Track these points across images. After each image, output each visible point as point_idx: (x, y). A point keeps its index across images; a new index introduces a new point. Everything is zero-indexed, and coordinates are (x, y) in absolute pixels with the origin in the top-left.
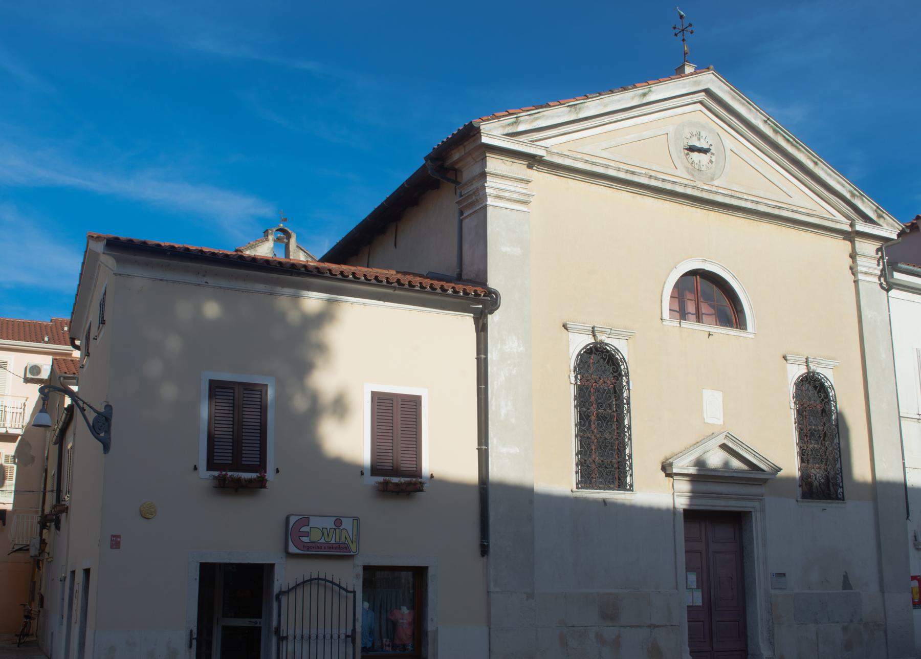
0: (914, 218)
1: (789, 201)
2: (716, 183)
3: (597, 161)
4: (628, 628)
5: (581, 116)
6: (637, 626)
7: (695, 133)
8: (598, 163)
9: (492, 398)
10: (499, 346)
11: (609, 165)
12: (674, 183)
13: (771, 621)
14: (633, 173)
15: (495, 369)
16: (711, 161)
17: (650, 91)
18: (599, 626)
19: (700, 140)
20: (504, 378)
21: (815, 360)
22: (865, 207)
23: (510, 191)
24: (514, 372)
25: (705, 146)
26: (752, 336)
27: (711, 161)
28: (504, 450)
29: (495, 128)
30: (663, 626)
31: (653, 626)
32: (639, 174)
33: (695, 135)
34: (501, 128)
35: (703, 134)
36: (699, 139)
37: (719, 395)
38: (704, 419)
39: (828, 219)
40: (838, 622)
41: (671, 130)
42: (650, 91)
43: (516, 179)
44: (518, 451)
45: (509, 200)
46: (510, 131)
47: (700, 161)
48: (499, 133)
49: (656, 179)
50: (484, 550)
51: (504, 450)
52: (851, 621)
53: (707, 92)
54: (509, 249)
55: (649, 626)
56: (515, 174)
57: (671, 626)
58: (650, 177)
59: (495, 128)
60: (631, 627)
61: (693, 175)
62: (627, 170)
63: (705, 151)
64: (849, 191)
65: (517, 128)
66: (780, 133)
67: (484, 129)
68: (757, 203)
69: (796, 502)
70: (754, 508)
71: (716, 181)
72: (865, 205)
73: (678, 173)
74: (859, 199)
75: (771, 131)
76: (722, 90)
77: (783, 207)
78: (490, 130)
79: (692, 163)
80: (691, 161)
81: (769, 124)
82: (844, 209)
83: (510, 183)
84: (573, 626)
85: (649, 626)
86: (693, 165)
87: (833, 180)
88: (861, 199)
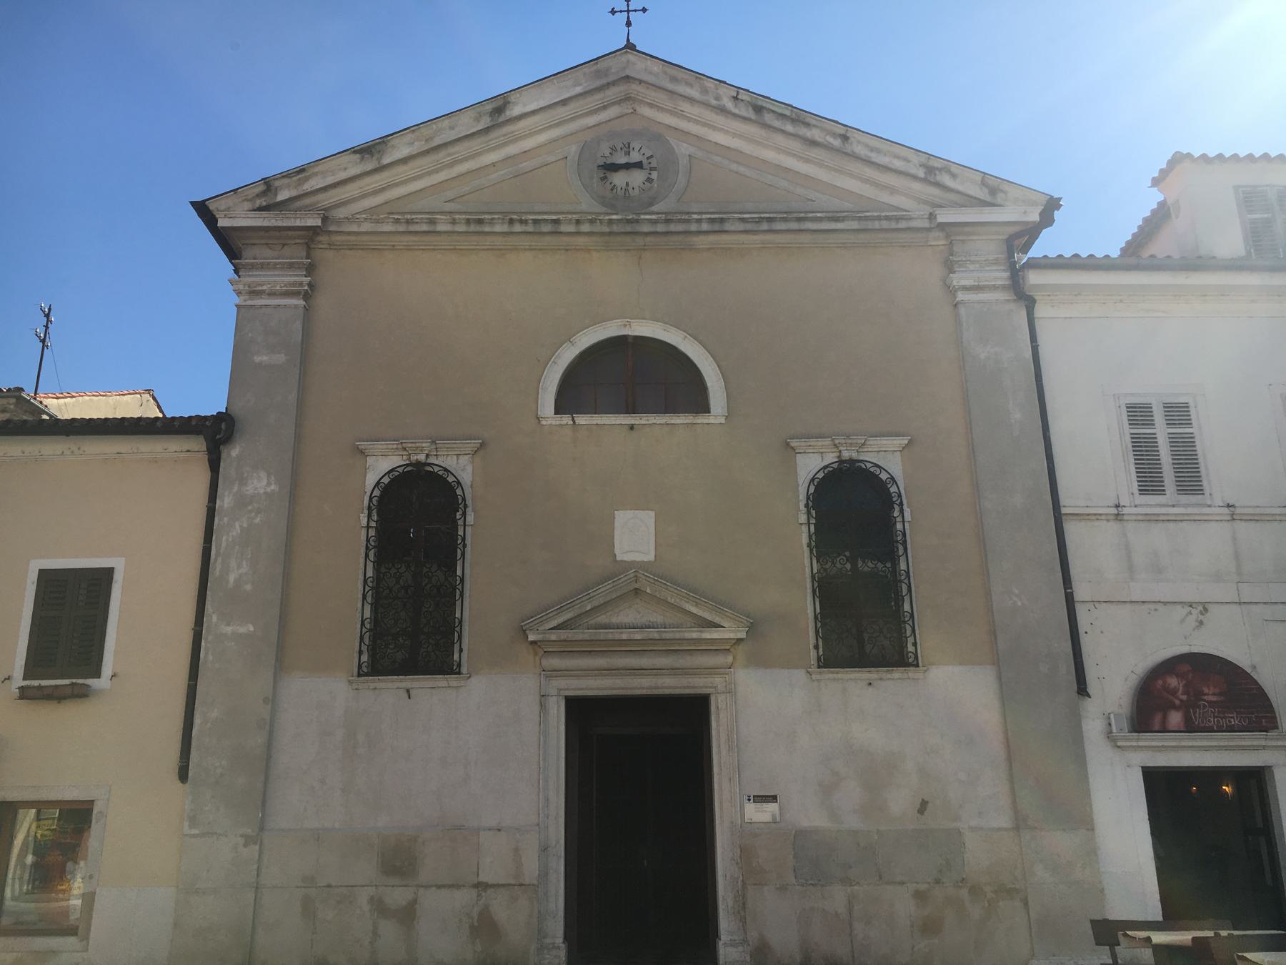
0: (1150, 185)
5: (386, 161)
7: (619, 146)
9: (216, 560)
10: (236, 488)
13: (741, 878)
15: (226, 519)
16: (649, 180)
17: (509, 103)
18: (376, 886)
19: (629, 154)
20: (239, 531)
24: (257, 520)
25: (635, 157)
26: (723, 420)
27: (649, 180)
28: (229, 629)
30: (503, 885)
31: (481, 886)
35: (636, 145)
36: (628, 153)
37: (648, 518)
38: (615, 555)
40: (902, 883)
41: (573, 150)
44: (252, 629)
47: (627, 184)
50: (183, 775)
51: (229, 629)
52: (938, 882)
54: (265, 358)
60: (439, 887)
63: (639, 165)
64: (921, 166)
65: (276, 199)
73: (584, 207)
75: (750, 109)
79: (612, 190)
80: (609, 187)
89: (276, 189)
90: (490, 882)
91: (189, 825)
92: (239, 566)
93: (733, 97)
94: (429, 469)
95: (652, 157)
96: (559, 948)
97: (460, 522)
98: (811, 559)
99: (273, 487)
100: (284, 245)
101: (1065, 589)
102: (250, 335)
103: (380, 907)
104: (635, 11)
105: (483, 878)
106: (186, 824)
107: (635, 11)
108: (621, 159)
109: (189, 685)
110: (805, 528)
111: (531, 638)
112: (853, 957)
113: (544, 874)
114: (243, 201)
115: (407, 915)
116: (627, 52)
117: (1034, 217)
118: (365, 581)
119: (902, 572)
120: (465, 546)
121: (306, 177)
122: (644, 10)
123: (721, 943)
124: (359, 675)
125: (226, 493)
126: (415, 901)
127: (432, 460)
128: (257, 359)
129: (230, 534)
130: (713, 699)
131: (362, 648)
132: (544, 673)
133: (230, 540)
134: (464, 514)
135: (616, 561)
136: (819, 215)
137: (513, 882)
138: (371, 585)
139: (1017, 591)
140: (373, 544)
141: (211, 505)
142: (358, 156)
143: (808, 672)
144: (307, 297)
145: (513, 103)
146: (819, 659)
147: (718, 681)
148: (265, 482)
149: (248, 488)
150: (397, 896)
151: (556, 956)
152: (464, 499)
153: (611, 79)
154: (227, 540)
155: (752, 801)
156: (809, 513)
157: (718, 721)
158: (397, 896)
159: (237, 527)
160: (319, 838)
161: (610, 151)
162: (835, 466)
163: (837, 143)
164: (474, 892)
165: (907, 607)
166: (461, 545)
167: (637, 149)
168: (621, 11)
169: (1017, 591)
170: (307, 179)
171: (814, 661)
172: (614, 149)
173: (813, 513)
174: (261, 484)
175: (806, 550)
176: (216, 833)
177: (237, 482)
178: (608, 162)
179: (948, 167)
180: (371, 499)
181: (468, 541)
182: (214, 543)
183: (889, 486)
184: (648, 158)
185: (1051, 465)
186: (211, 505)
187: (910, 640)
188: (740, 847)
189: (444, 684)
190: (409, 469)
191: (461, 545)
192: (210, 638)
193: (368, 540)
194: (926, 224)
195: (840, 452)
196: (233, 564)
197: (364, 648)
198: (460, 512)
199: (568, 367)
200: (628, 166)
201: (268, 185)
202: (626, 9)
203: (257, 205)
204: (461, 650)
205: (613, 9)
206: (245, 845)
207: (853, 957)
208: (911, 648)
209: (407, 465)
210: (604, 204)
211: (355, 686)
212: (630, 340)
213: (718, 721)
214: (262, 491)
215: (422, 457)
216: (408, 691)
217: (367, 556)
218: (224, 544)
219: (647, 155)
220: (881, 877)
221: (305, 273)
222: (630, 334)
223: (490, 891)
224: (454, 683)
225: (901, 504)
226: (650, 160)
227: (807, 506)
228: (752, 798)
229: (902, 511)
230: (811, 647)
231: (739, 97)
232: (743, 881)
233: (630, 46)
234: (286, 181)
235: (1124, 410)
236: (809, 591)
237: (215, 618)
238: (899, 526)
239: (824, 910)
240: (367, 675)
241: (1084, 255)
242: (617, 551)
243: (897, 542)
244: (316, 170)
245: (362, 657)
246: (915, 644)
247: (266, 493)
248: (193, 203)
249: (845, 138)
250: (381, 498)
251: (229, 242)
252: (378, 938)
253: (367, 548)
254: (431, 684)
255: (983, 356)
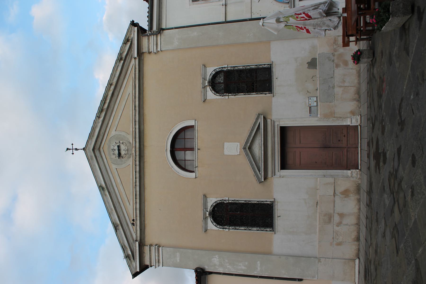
1: (131, 95)
2: (131, 142)
3: (135, 215)
4: (335, 208)
5: (119, 222)
6: (334, 203)
8: (135, 214)
9: (238, 272)
10: (217, 267)
11: (135, 208)
12: (136, 172)
13: (333, 118)
14: (136, 195)
15: (226, 270)
16: (123, 143)
17: (101, 186)
20: (230, 266)
21: (203, 83)
22: (125, 50)
23: (155, 257)
24: (227, 261)
25: (116, 148)
28: (259, 268)
29: (132, 266)
32: (136, 191)
33: (114, 152)
34: (132, 263)
35: (112, 147)
36: (115, 150)
37: (226, 145)
39: (135, 68)
40: (334, 71)
41: (114, 167)
42: (101, 186)
43: (150, 253)
45: (159, 256)
46: (132, 258)
47: (124, 150)
48: (134, 263)
49: (136, 182)
50: (300, 280)
51: (259, 268)
53: (93, 150)
54: (178, 259)
55: (334, 197)
56: (148, 263)
57: (334, 183)
58: (136, 185)
59: (132, 266)
60: (334, 206)
61: (131, 154)
62: (135, 198)
63: (119, 147)
64: (120, 62)
66: (102, 108)
67: (134, 271)
68: (135, 121)
69: (274, 97)
70: (278, 125)
71: (131, 141)
72: (125, 51)
73: (131, 163)
74: (122, 55)
75: (102, 113)
76: (91, 143)
77: (135, 105)
78: (134, 268)
79: (125, 155)
80: (125, 156)
81: (100, 115)
82: (129, 60)
83: (152, 255)
84: (333, 238)
85: (334, 197)
86: (126, 154)
87: (117, 72)
88: (122, 54)
89: (128, 254)
90: (333, 192)
91: (315, 278)
92: (240, 266)
93: (99, 118)
94: (211, 211)
95: (116, 143)
96: (352, 172)
97: (228, 201)
98: (239, 95)
99: (217, 256)
100: (144, 253)
101: (247, 21)
102: (171, 263)
103: (339, 224)
104: (73, 147)
105: (332, 194)
106: (314, 279)
107: (73, 147)
108: (117, 152)
109: (275, 279)
110: (230, 97)
111: (263, 180)
112: (354, 86)
113: (332, 176)
114: (132, 264)
115: (341, 215)
116: (85, 150)
117: (136, 28)
118: (245, 230)
119: (243, 68)
120: (235, 200)
121: (124, 246)
122: (72, 144)
123: (351, 125)
124: (273, 231)
125: (219, 270)
126: (338, 214)
127: (209, 210)
128: (178, 261)
129: (231, 268)
130: (281, 126)
131: (265, 230)
132: (273, 176)
133: (232, 268)
134: (225, 200)
135: (240, 155)
136: (134, 92)
137: (334, 185)
138: (246, 228)
139: (248, 35)
140: (234, 228)
141: (222, 274)
142: (118, 231)
143: (273, 96)
144: (159, 246)
145: (101, 184)
146: (269, 93)
147: (276, 124)
148: (215, 259)
149: (217, 263)
150: (336, 219)
151: (354, 173)
152: (221, 200)
153: (93, 155)
154: (232, 269)
155: (311, 114)
156: (225, 95)
157: (288, 124)
158: (336, 219)
159: (229, 266)
160: (319, 242)
161: (114, 155)
162: (210, 87)
163: (113, 87)
164: (336, 196)
165: (253, 67)
166: (234, 201)
167: (113, 147)
168: (73, 151)
169: (248, 35)
170: (125, 246)
171: (270, 95)
172: (114, 154)
173: (225, 94)
174: (216, 260)
175: (236, 96)
176: (317, 270)
177: (215, 267)
178: (118, 156)
179: (120, 54)
180: (221, 228)
181: (233, 199)
182: (233, 273)
183: (217, 71)
184: (116, 144)
185: (211, 24)
186: (222, 274)
187: (264, 66)
188: (324, 118)
189: (276, 206)
190: (211, 217)
191: (234, 201)
192: (261, 274)
193: (233, 229)
194: (137, 60)
195: (206, 86)
196: (240, 268)
197: (265, 230)
198: (224, 201)
199: (180, 169)
200: (119, 150)
201: (127, 257)
202: (72, 150)
203: (133, 260)
204: (266, 201)
205: (72, 154)
206: (321, 262)
207: (354, 86)
208: (266, 66)
209: (210, 217)
210: (130, 157)
211: (276, 232)
212: (171, 149)
213: (288, 124)
214: (218, 260)
215: (207, 213)
216: (278, 217)
217: (238, 229)
218: (234, 270)
219: (115, 144)
220: (332, 77)
221: (152, 247)
222: (170, 150)
223: (336, 192)
224: (276, 203)
225: (222, 68)
226: (117, 143)
227: (223, 96)
228: (310, 114)
229: (224, 68)
230: (265, 95)
231: (99, 116)
232: (334, 118)
233: (84, 149)
234: (125, 252)
235: (194, 3)
236: (249, 96)
237: (255, 272)
238: (229, 68)
239: (342, 94)
240: (273, 229)
241: (148, 14)
242: (237, 154)
243: (234, 69)
244: (122, 243)
245: (268, 230)
246: (265, 65)
247: (218, 258)
248: (133, 279)
249: (111, 85)
250: (220, 225)
251: (144, 268)
252: (348, 224)
253: (235, 229)
254: (276, 210)
255: (177, 43)
